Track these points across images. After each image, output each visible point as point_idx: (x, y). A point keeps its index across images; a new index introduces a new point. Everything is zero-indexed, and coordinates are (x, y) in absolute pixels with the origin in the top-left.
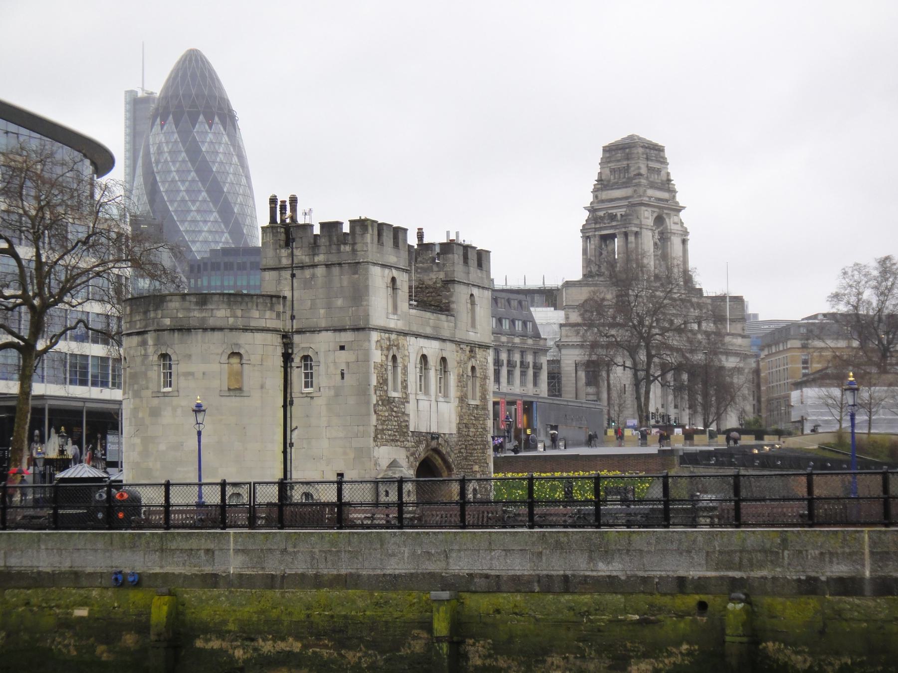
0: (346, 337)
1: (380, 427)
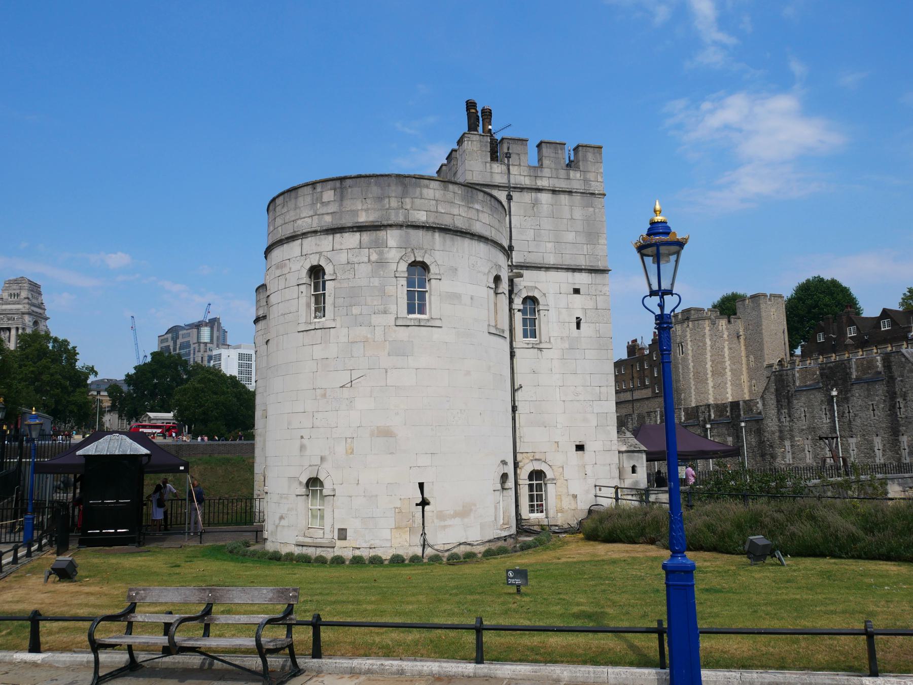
0: (582, 279)
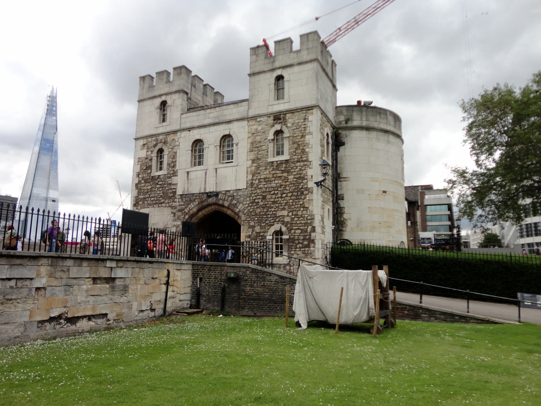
1: (142, 197)
